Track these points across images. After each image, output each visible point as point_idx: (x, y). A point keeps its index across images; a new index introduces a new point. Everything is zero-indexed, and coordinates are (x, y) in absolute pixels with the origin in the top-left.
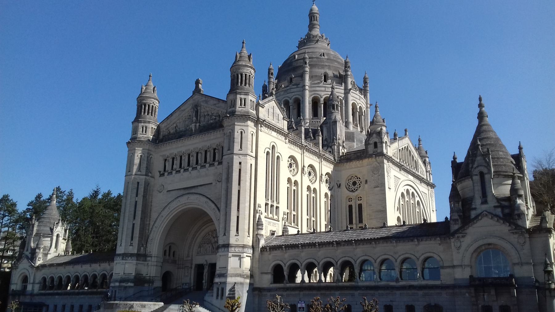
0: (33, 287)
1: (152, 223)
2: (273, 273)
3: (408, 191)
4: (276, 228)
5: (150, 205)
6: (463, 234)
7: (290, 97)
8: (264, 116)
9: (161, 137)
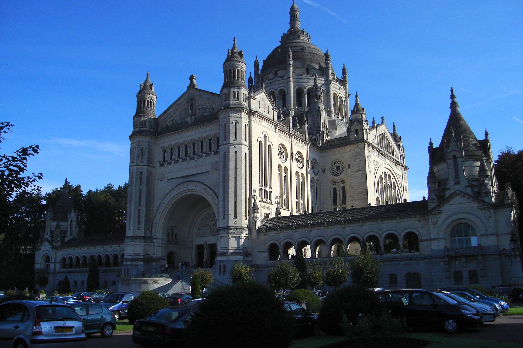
0: (55, 265)
1: (156, 209)
2: (269, 251)
3: (385, 172)
4: (270, 210)
6: (439, 211)
7: (276, 88)
8: (256, 107)
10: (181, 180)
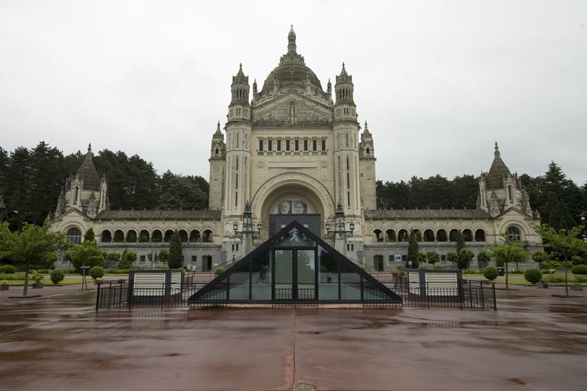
9: (255, 121)
10: (285, 171)
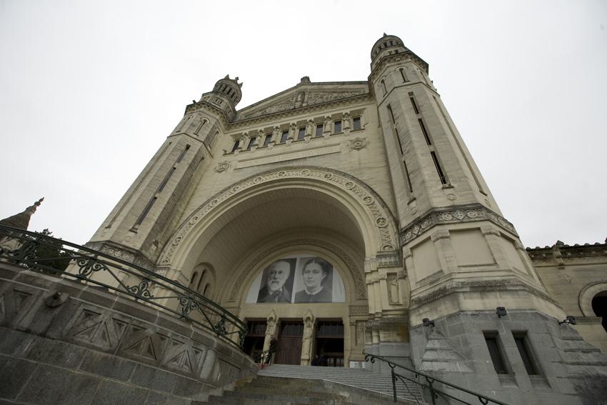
1: (188, 213)
5: (194, 186)
10: (268, 168)
